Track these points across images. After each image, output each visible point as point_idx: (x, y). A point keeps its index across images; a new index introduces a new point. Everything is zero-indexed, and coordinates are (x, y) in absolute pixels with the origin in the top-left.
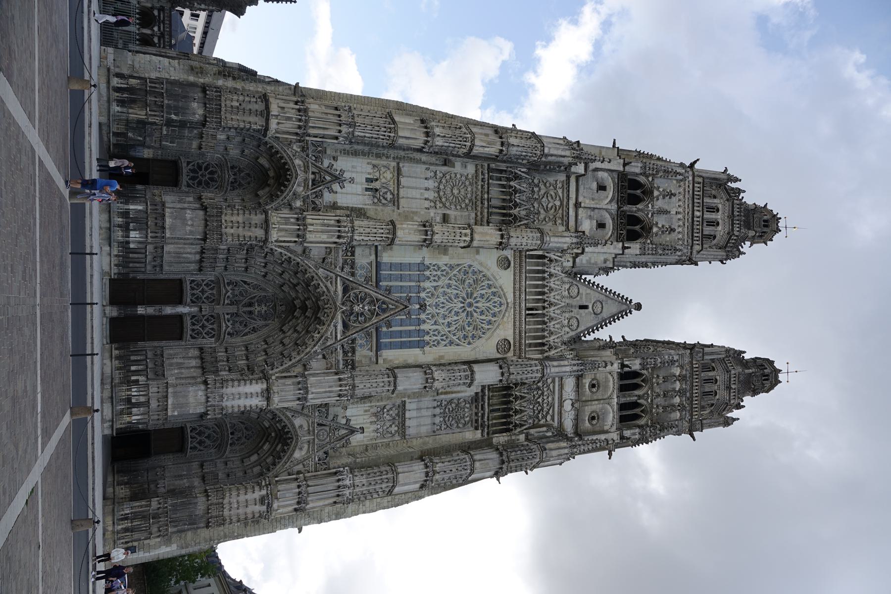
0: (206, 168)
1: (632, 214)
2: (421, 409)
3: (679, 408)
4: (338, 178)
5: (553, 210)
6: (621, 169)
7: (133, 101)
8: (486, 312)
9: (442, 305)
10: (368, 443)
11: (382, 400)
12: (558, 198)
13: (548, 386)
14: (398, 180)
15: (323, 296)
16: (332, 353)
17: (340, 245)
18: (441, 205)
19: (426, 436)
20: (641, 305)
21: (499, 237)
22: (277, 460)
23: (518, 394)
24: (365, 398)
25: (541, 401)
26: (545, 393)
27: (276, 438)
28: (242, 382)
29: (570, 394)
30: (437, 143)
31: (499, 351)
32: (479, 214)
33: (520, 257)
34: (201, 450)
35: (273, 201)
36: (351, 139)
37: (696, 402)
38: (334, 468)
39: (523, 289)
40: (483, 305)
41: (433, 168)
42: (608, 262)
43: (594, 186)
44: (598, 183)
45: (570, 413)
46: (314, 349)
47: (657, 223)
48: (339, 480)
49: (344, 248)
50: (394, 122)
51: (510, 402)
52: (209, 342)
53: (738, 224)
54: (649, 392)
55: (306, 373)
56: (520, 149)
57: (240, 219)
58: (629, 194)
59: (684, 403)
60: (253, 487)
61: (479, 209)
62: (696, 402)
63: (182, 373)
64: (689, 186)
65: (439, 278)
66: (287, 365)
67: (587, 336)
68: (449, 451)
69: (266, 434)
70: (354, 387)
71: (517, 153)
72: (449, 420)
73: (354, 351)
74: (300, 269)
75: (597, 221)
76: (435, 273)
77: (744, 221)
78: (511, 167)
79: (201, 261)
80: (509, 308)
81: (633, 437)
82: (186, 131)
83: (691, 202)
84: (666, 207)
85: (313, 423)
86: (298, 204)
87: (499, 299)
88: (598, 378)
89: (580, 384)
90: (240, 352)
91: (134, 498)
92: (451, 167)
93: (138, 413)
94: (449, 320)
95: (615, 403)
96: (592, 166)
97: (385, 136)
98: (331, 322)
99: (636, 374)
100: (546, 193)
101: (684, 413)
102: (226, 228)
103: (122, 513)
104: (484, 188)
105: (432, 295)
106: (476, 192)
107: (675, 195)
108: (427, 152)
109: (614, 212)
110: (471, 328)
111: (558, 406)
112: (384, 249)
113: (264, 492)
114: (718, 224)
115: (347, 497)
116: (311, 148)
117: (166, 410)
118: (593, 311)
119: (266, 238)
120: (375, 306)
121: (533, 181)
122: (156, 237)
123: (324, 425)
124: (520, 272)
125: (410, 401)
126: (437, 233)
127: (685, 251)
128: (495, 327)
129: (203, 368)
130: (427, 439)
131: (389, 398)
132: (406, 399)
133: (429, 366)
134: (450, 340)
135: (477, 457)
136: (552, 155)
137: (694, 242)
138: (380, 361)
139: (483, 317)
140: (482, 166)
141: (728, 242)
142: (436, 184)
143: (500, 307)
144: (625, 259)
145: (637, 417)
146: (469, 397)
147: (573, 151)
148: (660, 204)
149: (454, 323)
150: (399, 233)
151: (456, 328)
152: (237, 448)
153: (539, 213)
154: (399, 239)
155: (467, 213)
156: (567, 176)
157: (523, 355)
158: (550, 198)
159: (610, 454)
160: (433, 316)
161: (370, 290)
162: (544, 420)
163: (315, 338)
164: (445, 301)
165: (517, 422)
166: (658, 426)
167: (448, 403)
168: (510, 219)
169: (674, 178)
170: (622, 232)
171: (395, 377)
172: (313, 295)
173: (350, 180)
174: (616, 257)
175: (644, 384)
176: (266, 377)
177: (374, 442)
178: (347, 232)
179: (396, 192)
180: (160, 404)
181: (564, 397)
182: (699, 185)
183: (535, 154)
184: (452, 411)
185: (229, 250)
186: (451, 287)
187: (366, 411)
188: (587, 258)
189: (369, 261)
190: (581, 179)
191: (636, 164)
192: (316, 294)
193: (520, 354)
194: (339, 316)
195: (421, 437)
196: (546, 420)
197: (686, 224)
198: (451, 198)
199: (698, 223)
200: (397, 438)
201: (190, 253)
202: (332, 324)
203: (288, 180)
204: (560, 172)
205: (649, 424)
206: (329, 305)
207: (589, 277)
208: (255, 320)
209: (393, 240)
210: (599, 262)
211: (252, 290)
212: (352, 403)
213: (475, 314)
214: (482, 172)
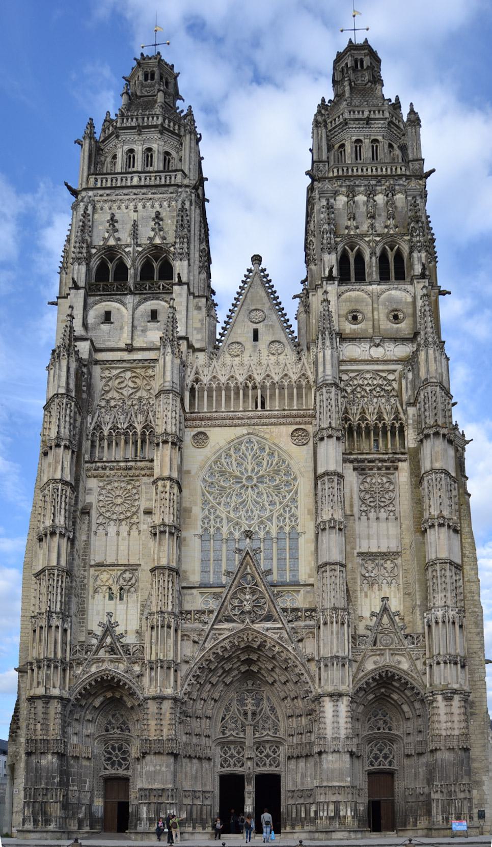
1: (139, 274)
2: (369, 534)
3: (390, 195)
4: (109, 629)
5: (137, 380)
7: (45, 813)
9: (250, 513)
10: (402, 593)
13: (352, 379)
14: (109, 566)
15: (234, 643)
16: (297, 633)
17: (178, 625)
18: (135, 517)
20: (254, 256)
22: (409, 686)
23: (358, 417)
24: (348, 596)
25: (370, 388)
26: (361, 382)
32: (143, 472)
36: (64, 615)
37: (384, 170)
38: (424, 628)
41: (94, 528)
42: (200, 304)
43: (105, 327)
44: (102, 323)
45: (387, 349)
46: (291, 651)
47: (150, 239)
49: (183, 621)
50: (43, 571)
53: (148, 118)
54: (367, 239)
55: (317, 659)
57: (153, 723)
58: (115, 279)
59: (384, 187)
60: (433, 708)
61: (137, 472)
62: (384, 170)
63: (311, 774)
64: (101, 196)
65: (218, 517)
66: (308, 677)
68: (420, 500)
69: (383, 696)
72: (384, 502)
74: (206, 666)
75: (149, 322)
76: (212, 522)
77: (146, 109)
78: (87, 435)
80: (254, 432)
81: (424, 260)
84: (129, 227)
85: (372, 651)
86: (137, 668)
88: (345, 312)
89: (350, 336)
90: (294, 722)
91: (429, 812)
92: (91, 506)
93: (345, 810)
94: (267, 504)
95: (379, 287)
96: (79, 330)
98: (263, 634)
99: (343, 261)
100: (118, 390)
101: (397, 187)
102: (162, 736)
103: (441, 822)
104: (114, 466)
106: (119, 476)
107: (113, 215)
108: (74, 533)
109: (137, 298)
111: (378, 364)
112: (186, 579)
116: (78, 655)
118: (260, 322)
120: (246, 588)
121: (103, 407)
122: (172, 796)
124: (209, 419)
125: (358, 547)
127: (184, 195)
128: (276, 448)
129: (307, 756)
130: (404, 526)
131: (353, 571)
132: (355, 552)
133: (317, 527)
135: (428, 467)
137: (173, 183)
138: (311, 581)
139: (265, 463)
140: (88, 470)
141: (173, 133)
142: (112, 523)
144: (196, 281)
145: (399, 256)
146: (358, 478)
150: (164, 562)
152: (394, 724)
153: (140, 399)
155: (143, 487)
156: (95, 364)
158: (123, 385)
162: (394, 383)
164: (244, 509)
165: (393, 417)
166: (412, 225)
167: (364, 503)
168: (147, 433)
169: (90, 218)
170: (161, 287)
171: (326, 564)
172: (234, 653)
174: (193, 294)
175: (357, 248)
177: (401, 586)
179: (122, 568)
181: (367, 357)
182: (99, 181)
185: (187, 734)
186: (228, 503)
187: (366, 596)
188: (195, 332)
190: (98, 346)
191: (75, 272)
192: (233, 650)
193: (309, 416)
194: (257, 626)
195: (401, 534)
197: (150, 196)
198: (126, 505)
199: (148, 178)
203: (113, 678)
204: (90, 374)
205: (408, 238)
206: (245, 637)
207: (219, 330)
212: (354, 610)
213: (261, 473)
214: (95, 470)
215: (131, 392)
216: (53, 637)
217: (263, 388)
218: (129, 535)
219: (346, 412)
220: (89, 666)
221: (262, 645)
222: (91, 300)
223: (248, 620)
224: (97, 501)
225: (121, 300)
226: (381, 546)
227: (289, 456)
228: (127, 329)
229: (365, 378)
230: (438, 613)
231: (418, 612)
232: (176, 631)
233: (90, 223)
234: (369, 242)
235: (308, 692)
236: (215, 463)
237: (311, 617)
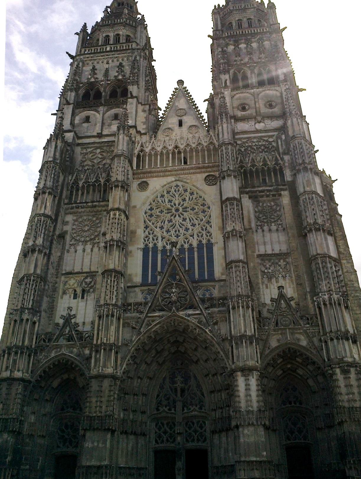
0: (63, 431)
4: (68, 319)
5: (104, 154)
6: (71, 107)
8: (184, 197)
11: (256, 274)
12: (95, 151)
18: (97, 239)
19: (288, 234)
21: (117, 189)
24: (251, 286)
26: (250, 144)
27: (292, 363)
28: (237, 393)
29: (250, 125)
30: (41, 243)
34: (307, 432)
35: (84, 374)
38: (315, 310)
40: (177, 200)
41: (67, 248)
43: (85, 125)
45: (266, 123)
47: (115, 77)
48: (325, 304)
51: (257, 170)
52: (208, 427)
54: (248, 65)
55: (229, 338)
56: (48, 179)
59: (256, 39)
60: (333, 381)
61: (100, 209)
65: (155, 236)
66: (223, 355)
67: (205, 121)
70: (239, 296)
71: (52, 181)
72: (273, 218)
73: (211, 299)
74: (141, 348)
76: (151, 239)
79: (135, 434)
80: (180, 179)
82: (27, 448)
83: (99, 55)
84: (103, 72)
87: (172, 188)
95: (258, 90)
97: (33, 284)
98: (185, 319)
104: (84, 206)
105: (168, 240)
106: (87, 212)
108: (50, 251)
109: (106, 108)
111: (261, 133)
112: (130, 280)
113: (338, 371)
114: (118, 35)
115: (341, 296)
117: (261, 462)
119: (111, 377)
120: (173, 284)
122: (106, 473)
123: (277, 320)
124: (150, 172)
125: (257, 251)
126: (112, 237)
127: (136, 53)
128: (195, 188)
130: (290, 234)
132: (255, 254)
133: (224, 237)
134: (206, 223)
136: (55, 154)
138: (224, 277)
139: (187, 199)
143: (179, 186)
146: (253, 204)
147: (52, 140)
148: (100, 76)
149: (192, 221)
150: (111, 267)
151: (196, 219)
157: (217, 164)
159: (302, 90)
160: (187, 239)
163: (200, 332)
167: (259, 220)
173: (69, 310)
176: (233, 372)
179: (85, 275)
180: (255, 468)
181: (253, 129)
183: (53, 167)
184: (266, 216)
187: (267, 287)
194: (181, 313)
195: (289, 240)
196: (272, 142)
197: (116, 56)
198: (91, 231)
200: (290, 260)
201: (127, 444)
204: (73, 151)
206: (172, 322)
208: (190, 386)
210: (145, 115)
211: (164, 390)
215: (99, 161)
216: (23, 328)
217: (185, 152)
218: (92, 251)
219: (241, 161)
220: (50, 352)
221: (185, 330)
222: (77, 111)
223: (174, 308)
224: (71, 229)
225: (95, 110)
226: (275, 249)
228: (99, 125)
229: (253, 142)
230: (325, 297)
231: (309, 297)
232: (119, 319)
233: (80, 71)
234: (249, 67)
235: (224, 368)
237: (223, 305)
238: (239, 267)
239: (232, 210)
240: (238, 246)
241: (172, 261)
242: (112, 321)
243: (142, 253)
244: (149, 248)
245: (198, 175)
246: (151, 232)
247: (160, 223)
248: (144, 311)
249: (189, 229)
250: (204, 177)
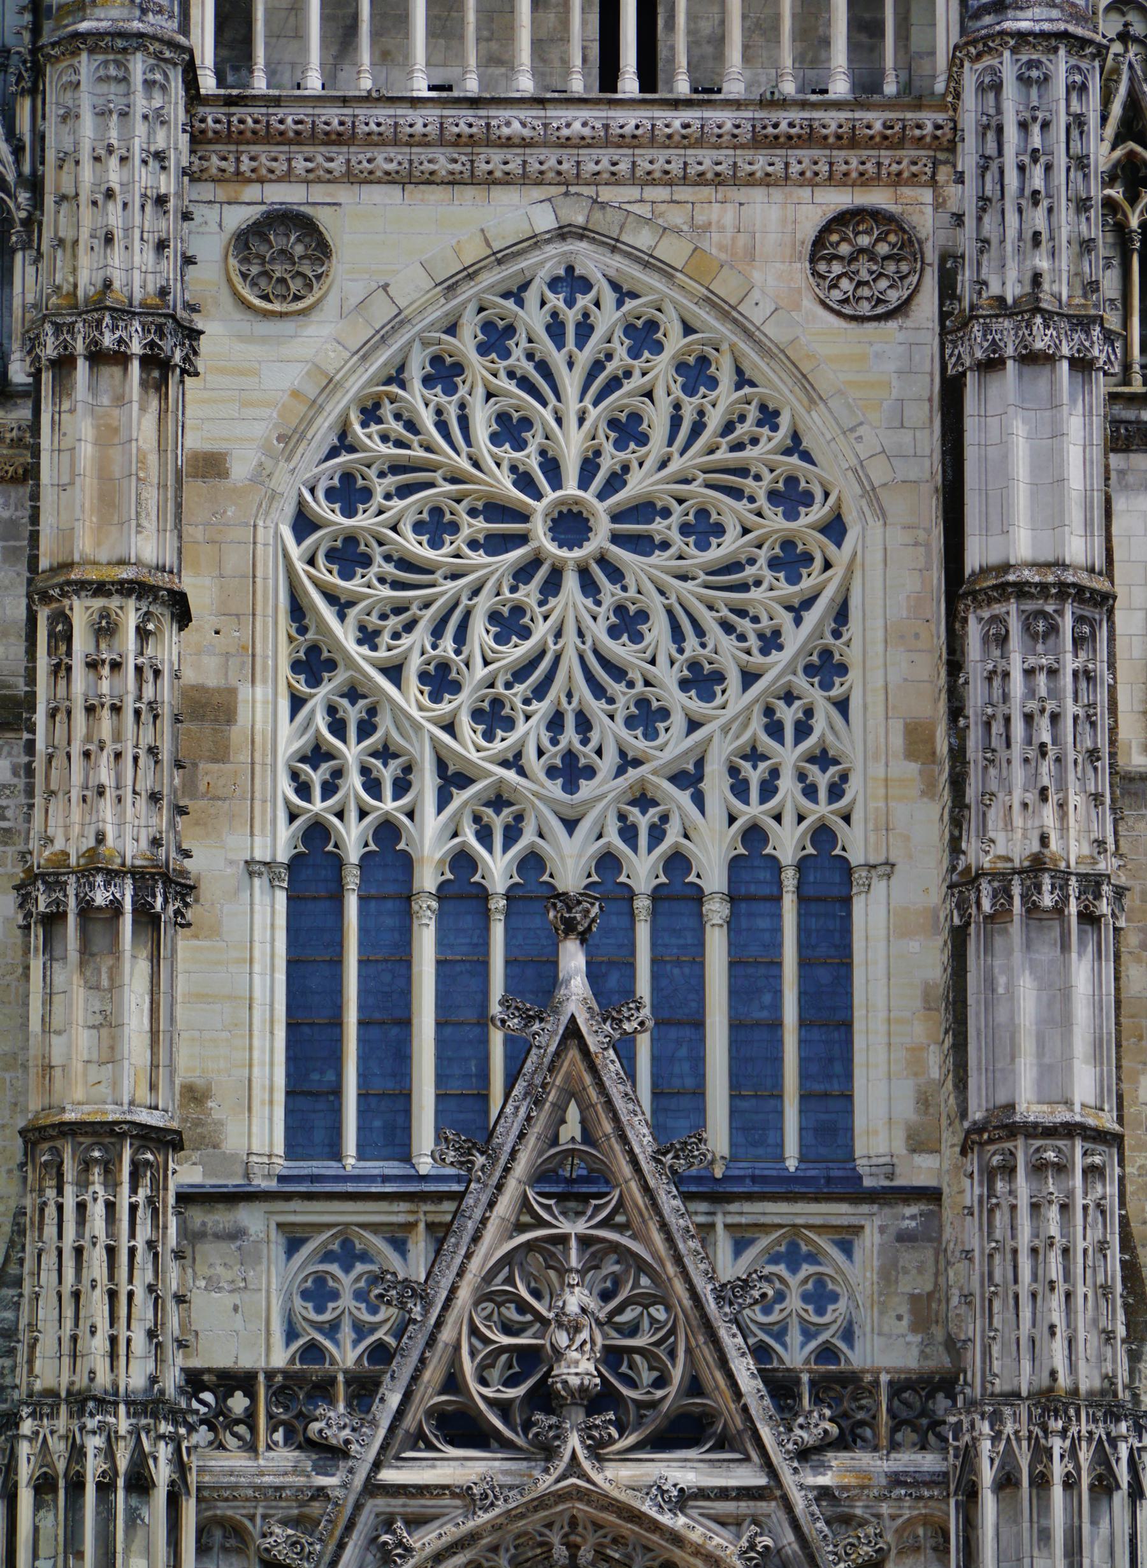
9: (570, 736)
16: (847, 1520)
31: (894, 297)
33: (235, 138)
39: (463, 121)
40: (572, 420)
65: (385, 753)
76: (354, 780)
80: (605, 222)
87: (531, 296)
94: (668, 676)
98: (656, 1527)
105: (498, 802)
110: (730, 511)
120: (563, 1239)
128: (724, 330)
134: (810, 670)
139: (657, 419)
143: (586, 285)
149: (691, 642)
151: (728, 628)
154: (143, 1094)
157: (929, 118)
160: (644, 801)
161: (460, 1274)
164: (542, 708)
178: (112, 1438)
186: (444, 667)
189: (277, 1248)
202: (666, 1519)
206: (555, 1539)
209: (148, 1136)
213: (637, 485)
223: (574, 1441)
227: (804, 380)
236: (370, 414)
238: (1062, 1169)
239: (1042, 679)
240: (1065, 993)
241: (557, 1054)
242: (133, 1518)
243: (281, 897)
244: (337, 862)
245: (758, 194)
246: (353, 714)
247: (420, 636)
248: (354, 1447)
249: (664, 713)
250: (809, 230)
